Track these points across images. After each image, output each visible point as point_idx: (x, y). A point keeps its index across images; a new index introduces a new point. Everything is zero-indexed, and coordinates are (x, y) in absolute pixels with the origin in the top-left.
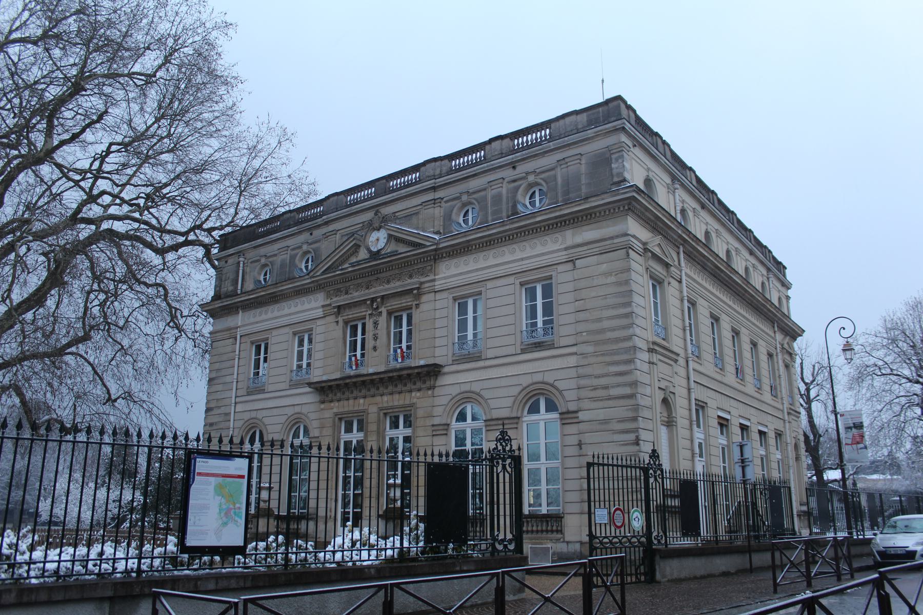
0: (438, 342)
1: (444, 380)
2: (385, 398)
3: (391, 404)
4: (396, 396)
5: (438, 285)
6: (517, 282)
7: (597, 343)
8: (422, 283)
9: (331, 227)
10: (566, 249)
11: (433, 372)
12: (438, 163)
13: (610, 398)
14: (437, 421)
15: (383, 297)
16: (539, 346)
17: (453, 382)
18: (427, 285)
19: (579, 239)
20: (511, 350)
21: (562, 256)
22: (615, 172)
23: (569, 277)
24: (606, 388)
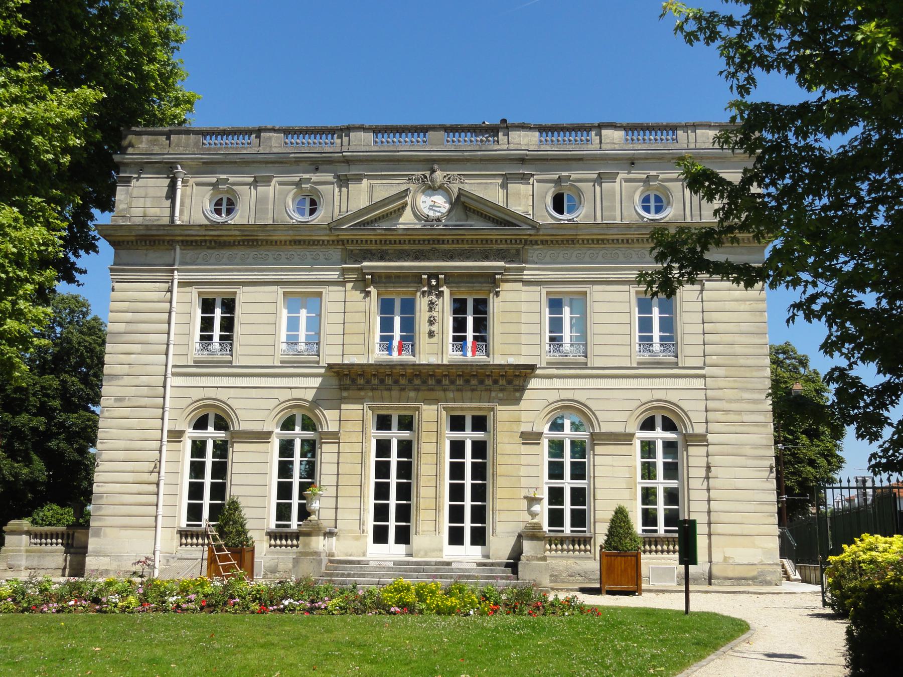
14: (526, 428)
24: (739, 412)
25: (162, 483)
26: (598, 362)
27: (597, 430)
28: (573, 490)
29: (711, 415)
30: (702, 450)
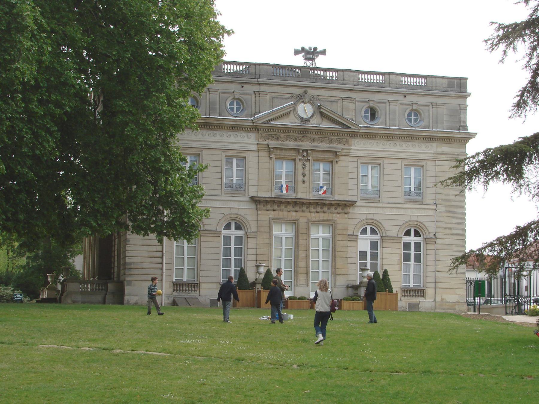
0: (350, 187)
1: (352, 210)
2: (313, 215)
3: (317, 218)
4: (322, 215)
5: (352, 153)
6: (403, 164)
7: (447, 206)
8: (343, 149)
9: (263, 88)
10: (433, 154)
11: (352, 204)
12: (352, 73)
13: (453, 234)
14: (350, 233)
15: (311, 150)
16: (414, 202)
17: (361, 212)
18: (345, 151)
19: (440, 150)
20: (398, 201)
21: (431, 157)
22: (462, 119)
23: (433, 168)
24: (451, 229)
25: (164, 257)
26: (385, 200)
27: (384, 235)
28: (236, 237)
29: (438, 230)
30: (432, 247)
